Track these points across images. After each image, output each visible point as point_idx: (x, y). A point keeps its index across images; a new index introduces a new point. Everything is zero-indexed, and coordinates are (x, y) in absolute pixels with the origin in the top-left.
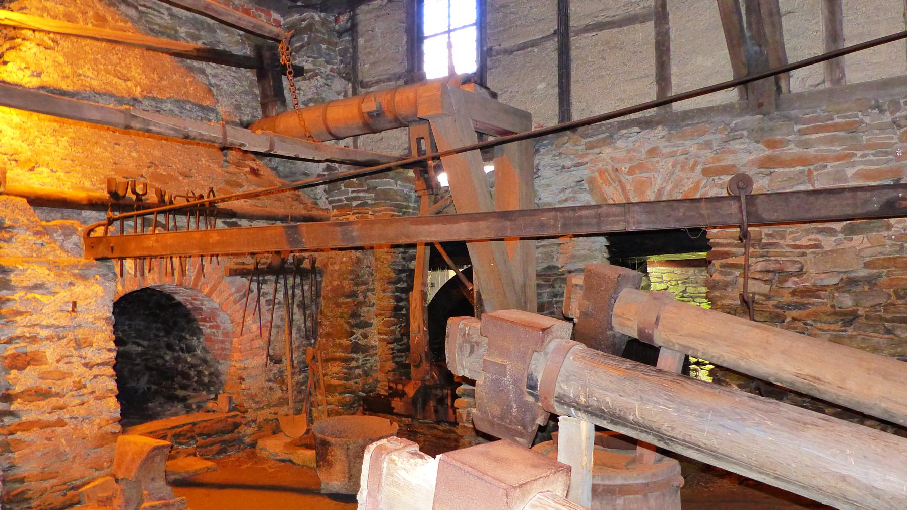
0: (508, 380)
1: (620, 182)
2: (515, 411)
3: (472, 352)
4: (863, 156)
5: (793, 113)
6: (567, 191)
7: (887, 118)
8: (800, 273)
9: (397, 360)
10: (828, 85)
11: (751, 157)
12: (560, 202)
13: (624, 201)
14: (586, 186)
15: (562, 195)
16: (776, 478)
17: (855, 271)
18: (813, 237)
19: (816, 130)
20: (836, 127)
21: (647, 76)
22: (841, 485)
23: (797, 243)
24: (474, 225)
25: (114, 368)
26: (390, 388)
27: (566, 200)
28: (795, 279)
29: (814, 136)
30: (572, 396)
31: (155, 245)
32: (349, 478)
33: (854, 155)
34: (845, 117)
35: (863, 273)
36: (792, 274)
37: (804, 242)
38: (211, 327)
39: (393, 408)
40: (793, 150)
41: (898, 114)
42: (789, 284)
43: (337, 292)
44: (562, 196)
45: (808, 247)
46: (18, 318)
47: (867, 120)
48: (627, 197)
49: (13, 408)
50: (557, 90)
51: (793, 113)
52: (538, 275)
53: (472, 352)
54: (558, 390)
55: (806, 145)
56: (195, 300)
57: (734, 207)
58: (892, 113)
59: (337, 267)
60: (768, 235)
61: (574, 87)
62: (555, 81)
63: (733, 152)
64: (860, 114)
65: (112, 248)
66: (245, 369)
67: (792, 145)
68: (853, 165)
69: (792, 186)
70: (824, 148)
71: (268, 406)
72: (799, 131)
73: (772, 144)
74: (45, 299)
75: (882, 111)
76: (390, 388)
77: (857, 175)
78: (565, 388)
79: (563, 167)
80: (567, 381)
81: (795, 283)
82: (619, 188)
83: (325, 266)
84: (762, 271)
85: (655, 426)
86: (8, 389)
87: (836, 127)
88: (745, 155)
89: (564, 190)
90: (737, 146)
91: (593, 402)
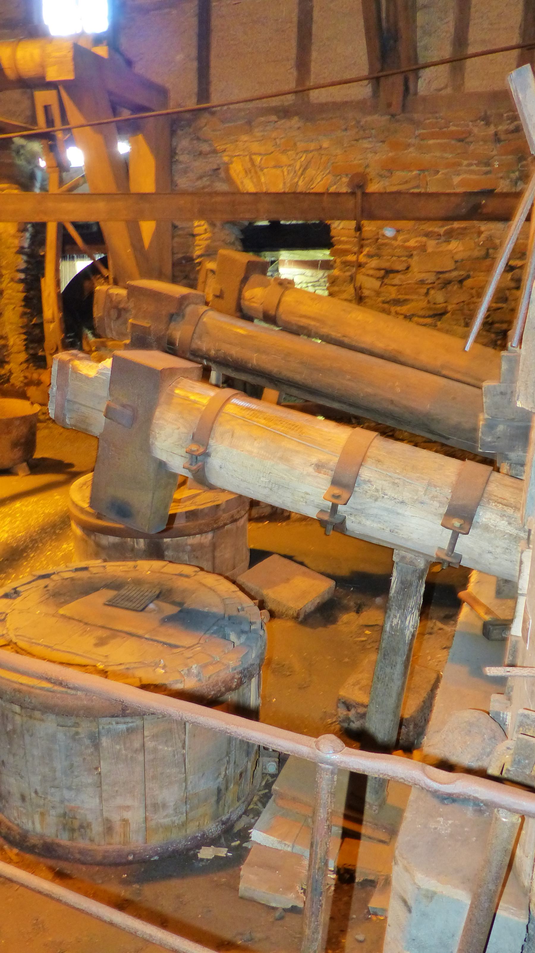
3: (119, 316)
5: (416, 116)
6: (205, 179)
7: (492, 130)
10: (449, 90)
11: (377, 157)
16: (351, 405)
18: (419, 239)
19: (433, 136)
22: (391, 407)
26: (26, 377)
29: (431, 142)
30: (204, 349)
33: (460, 164)
34: (457, 126)
35: (455, 274)
37: (412, 243)
40: (412, 154)
41: (500, 128)
44: (199, 184)
45: (415, 248)
47: (476, 130)
51: (416, 116)
52: (174, 265)
53: (119, 316)
54: (194, 346)
57: (350, 203)
62: (194, 52)
64: (471, 123)
67: (411, 149)
72: (419, 135)
75: (488, 124)
76: (26, 377)
78: (199, 343)
79: (201, 153)
88: (370, 156)
89: (201, 178)
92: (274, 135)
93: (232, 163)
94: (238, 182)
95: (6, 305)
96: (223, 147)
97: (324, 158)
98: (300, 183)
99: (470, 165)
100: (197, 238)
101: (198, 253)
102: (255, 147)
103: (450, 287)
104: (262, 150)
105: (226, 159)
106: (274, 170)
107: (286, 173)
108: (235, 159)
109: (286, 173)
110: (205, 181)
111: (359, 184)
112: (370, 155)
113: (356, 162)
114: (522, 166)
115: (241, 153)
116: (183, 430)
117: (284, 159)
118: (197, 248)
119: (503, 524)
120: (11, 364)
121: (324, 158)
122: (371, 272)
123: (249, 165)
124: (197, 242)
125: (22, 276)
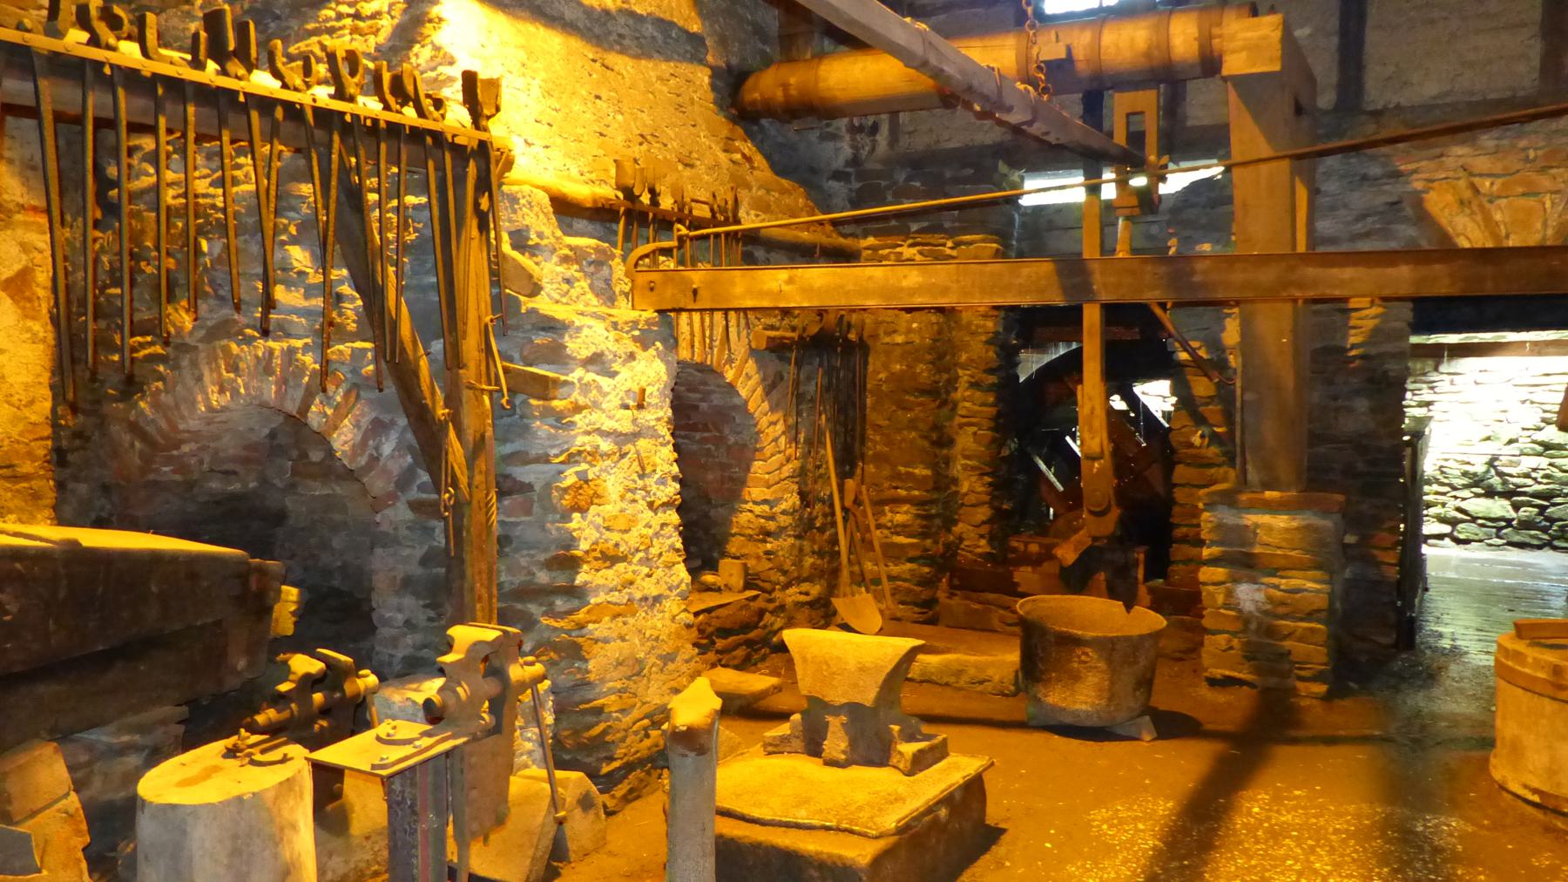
1: (1481, 206)
6: (1370, 220)
9: (996, 504)
13: (1489, 244)
14: (1409, 211)
21: (1523, 25)
24: (1424, 271)
25: (679, 510)
27: (1367, 235)
31: (785, 288)
32: (1110, 699)
38: (704, 440)
39: (1017, 584)
43: (903, 386)
44: (1359, 227)
46: (577, 418)
48: (1495, 236)
49: (580, 579)
50: (1335, 40)
56: (688, 390)
59: (899, 339)
61: (1372, 37)
62: (1334, 23)
65: (695, 292)
66: (772, 518)
71: (800, 580)
74: (604, 381)
79: (1365, 178)
82: (1479, 218)
83: (875, 336)
86: (569, 547)
89: (1362, 217)
92: (1523, 143)
93: (1426, 191)
94: (1444, 221)
95: (961, 426)
96: (1411, 167)
100: (1354, 314)
101: (1353, 340)
102: (1482, 163)
104: (1498, 168)
105: (1418, 185)
106: (1522, 201)
107: (1548, 205)
108: (1436, 184)
109: (1548, 205)
115: (1451, 174)
117: (1545, 182)
118: (1353, 332)
120: (961, 525)
123: (1468, 194)
124: (1352, 323)
125: (993, 379)
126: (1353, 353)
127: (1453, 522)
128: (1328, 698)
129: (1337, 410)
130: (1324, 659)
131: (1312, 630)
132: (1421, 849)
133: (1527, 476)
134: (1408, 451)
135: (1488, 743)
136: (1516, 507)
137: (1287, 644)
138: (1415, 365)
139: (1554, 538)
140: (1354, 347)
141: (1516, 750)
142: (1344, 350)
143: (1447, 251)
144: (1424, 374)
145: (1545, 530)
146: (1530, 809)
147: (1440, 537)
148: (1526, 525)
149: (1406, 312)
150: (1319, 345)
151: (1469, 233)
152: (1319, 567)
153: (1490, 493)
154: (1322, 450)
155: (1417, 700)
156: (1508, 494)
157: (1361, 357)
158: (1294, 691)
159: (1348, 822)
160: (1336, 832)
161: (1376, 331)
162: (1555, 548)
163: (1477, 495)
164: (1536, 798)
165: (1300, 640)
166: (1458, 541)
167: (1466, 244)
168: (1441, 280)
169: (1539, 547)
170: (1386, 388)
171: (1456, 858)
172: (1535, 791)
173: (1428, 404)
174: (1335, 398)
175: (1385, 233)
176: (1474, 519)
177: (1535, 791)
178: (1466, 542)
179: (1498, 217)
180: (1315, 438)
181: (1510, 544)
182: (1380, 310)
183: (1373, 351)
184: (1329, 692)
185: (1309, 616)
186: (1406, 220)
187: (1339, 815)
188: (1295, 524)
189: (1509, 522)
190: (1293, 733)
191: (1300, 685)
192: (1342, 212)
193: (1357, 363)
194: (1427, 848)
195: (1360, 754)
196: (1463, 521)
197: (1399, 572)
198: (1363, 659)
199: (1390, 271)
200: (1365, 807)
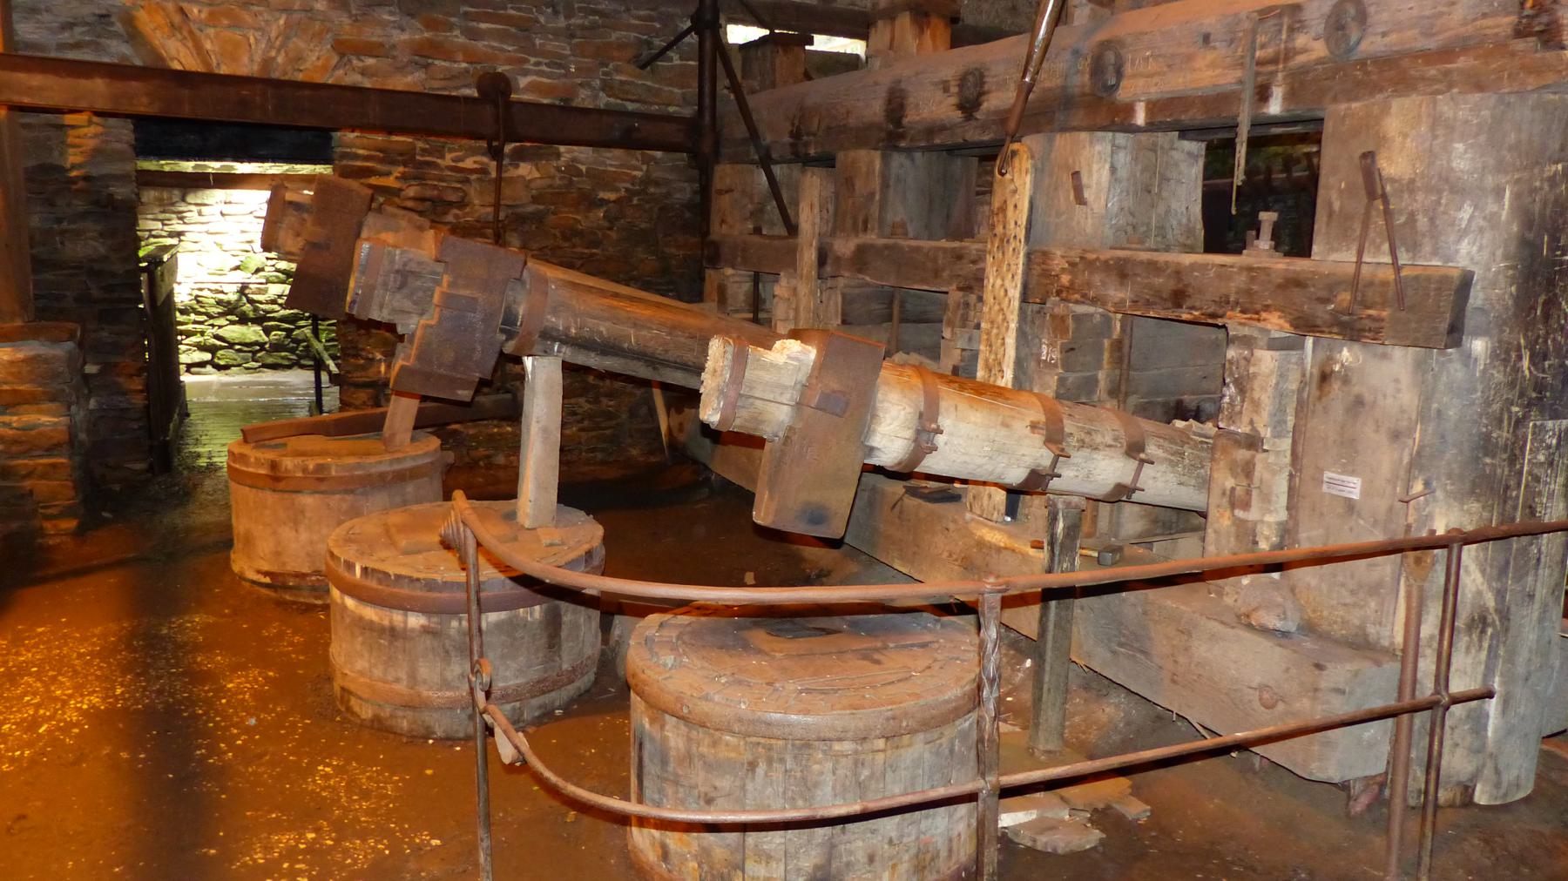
0: (476, 317)
1: (191, 32)
2: (477, 356)
4: (538, 64)
6: (78, 30)
7: (562, 22)
8: (462, 204)
11: (405, 37)
12: (62, 46)
13: (201, 69)
14: (118, 27)
15: (66, 35)
17: (522, 206)
18: (478, 158)
20: (509, 20)
23: (460, 165)
24: (119, 86)
27: (77, 46)
28: (456, 211)
29: (483, 26)
34: (519, 9)
35: (531, 208)
36: (451, 204)
37: (469, 163)
42: (450, 218)
44: (65, 37)
47: (542, 19)
48: (207, 63)
55: (474, 35)
58: (568, 17)
60: (423, 150)
63: (384, 24)
67: (457, 32)
68: (526, 73)
69: (457, 88)
70: (495, 44)
72: (466, 13)
73: (431, 25)
75: (556, 13)
77: (532, 87)
80: (555, 312)
81: (456, 216)
82: (190, 44)
84: (414, 199)
85: (649, 351)
87: (509, 20)
90: (386, 17)
91: (586, 333)
97: (317, 25)
98: (280, 60)
99: (538, 64)
100: (71, 132)
103: (526, 228)
106: (228, 34)
109: (252, 40)
110: (78, 33)
111: (496, 88)
112: (395, 32)
113: (374, 39)
114: (605, 74)
116: (908, 410)
118: (71, 151)
119: (1160, 453)
121: (317, 25)
122: (410, 204)
123: (177, 19)
124: (70, 140)
126: (74, 174)
127: (213, 350)
128: (79, 534)
129: (63, 233)
130: (72, 493)
131: (53, 466)
132: (165, 650)
133: (273, 302)
134: (144, 277)
135: (228, 544)
136: (267, 331)
137: (27, 484)
138: (149, 195)
139: (300, 357)
140: (74, 167)
141: (249, 540)
142: (62, 170)
143: (158, 73)
144: (173, 204)
145: (292, 351)
146: (264, 591)
147: (202, 364)
148: (277, 347)
149: (125, 133)
150: (31, 163)
151: (181, 57)
152: (53, 399)
153: (244, 320)
154: (49, 276)
155: (174, 518)
156: (259, 320)
157: (86, 178)
158: (41, 532)
159: (94, 644)
160: (80, 656)
161: (97, 152)
162: (303, 367)
163: (232, 323)
164: (267, 580)
165: (43, 476)
166: (219, 368)
167: (176, 66)
168: (143, 100)
169: (289, 367)
170: (120, 220)
171: (197, 648)
172: (266, 574)
173: (179, 234)
174: (59, 221)
175: (96, 46)
176: (231, 345)
177: (266, 574)
178: (226, 367)
179: (208, 46)
180: (39, 264)
181: (264, 366)
182: (100, 129)
183: (94, 172)
184: (80, 526)
185: (51, 450)
186: (116, 35)
187: (84, 639)
188: (20, 355)
189: (262, 345)
190: (51, 572)
191: (48, 525)
192: (46, 17)
193: (81, 184)
194: (170, 646)
195: (111, 579)
196: (222, 348)
197: (147, 398)
198: (117, 487)
199: (83, 82)
200: (113, 626)
